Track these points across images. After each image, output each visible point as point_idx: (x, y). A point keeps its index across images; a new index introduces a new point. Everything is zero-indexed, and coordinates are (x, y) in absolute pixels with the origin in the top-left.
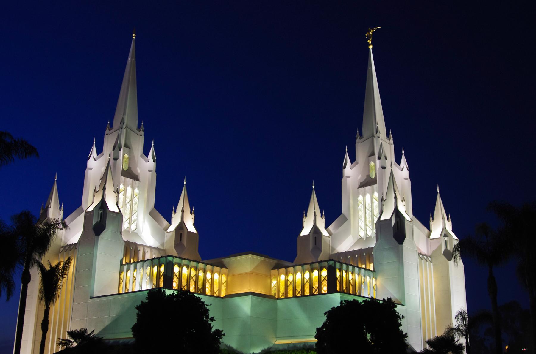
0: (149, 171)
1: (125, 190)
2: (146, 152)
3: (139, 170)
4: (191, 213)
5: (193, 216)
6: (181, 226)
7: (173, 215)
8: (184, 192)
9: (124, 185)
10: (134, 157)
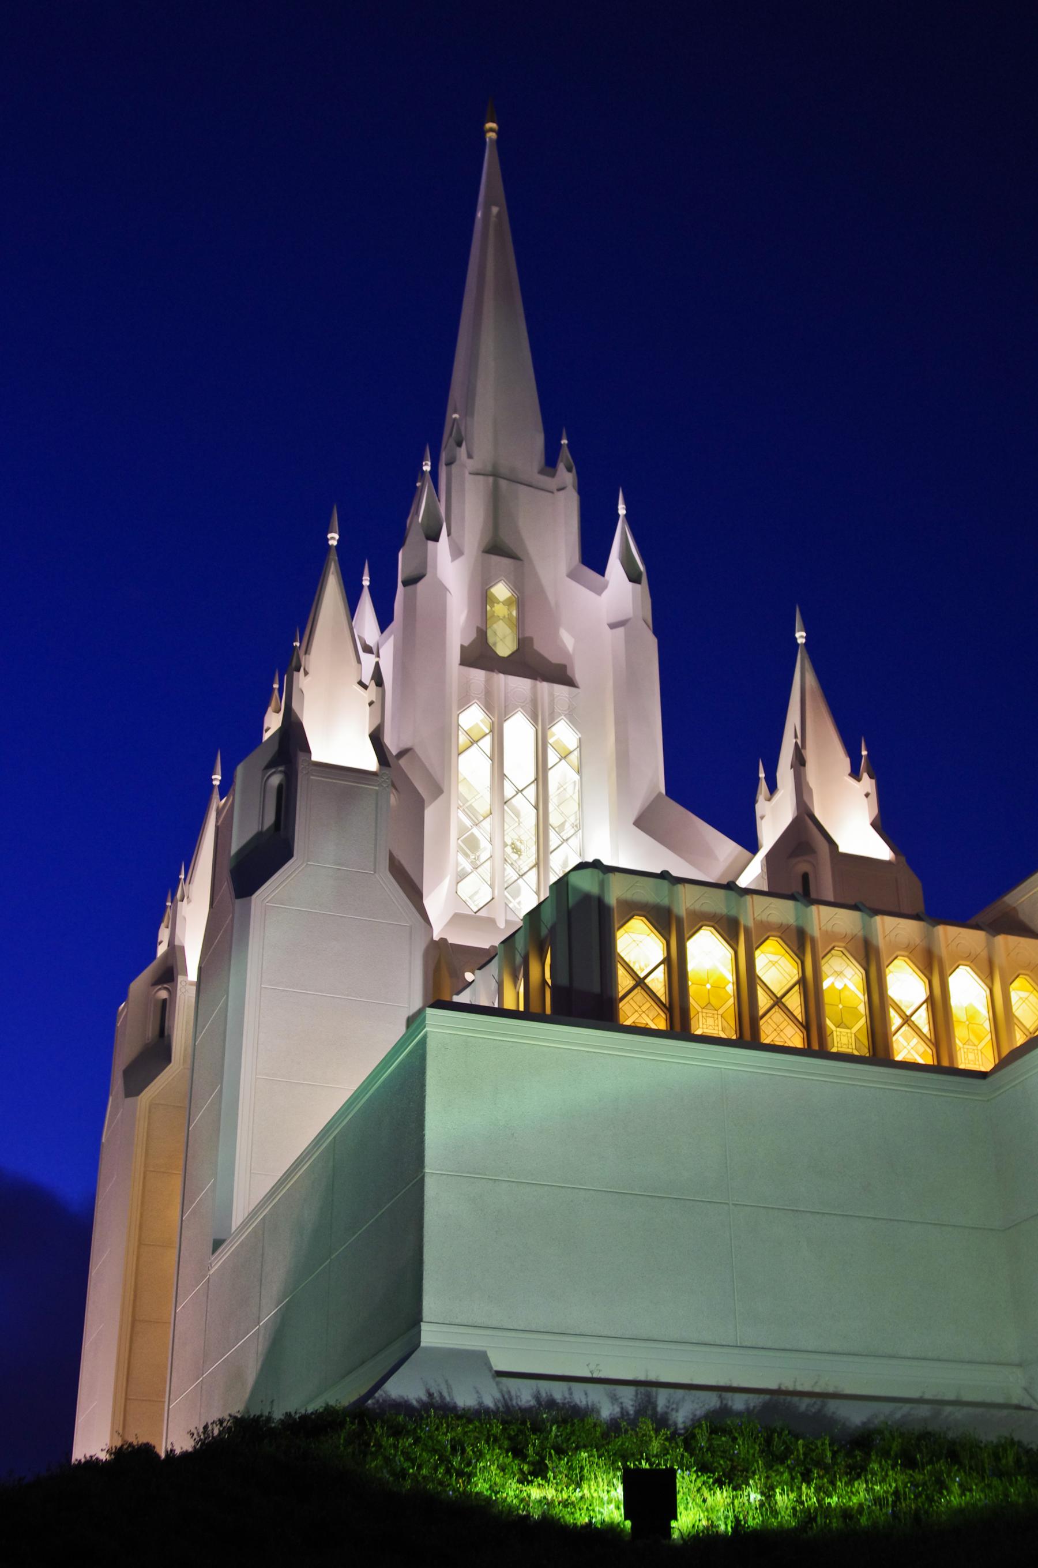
0: (613, 626)
2: (594, 556)
3: (568, 640)
4: (855, 774)
5: (868, 784)
6: (805, 834)
7: (762, 806)
8: (803, 680)
9: (488, 707)
10: (540, 590)
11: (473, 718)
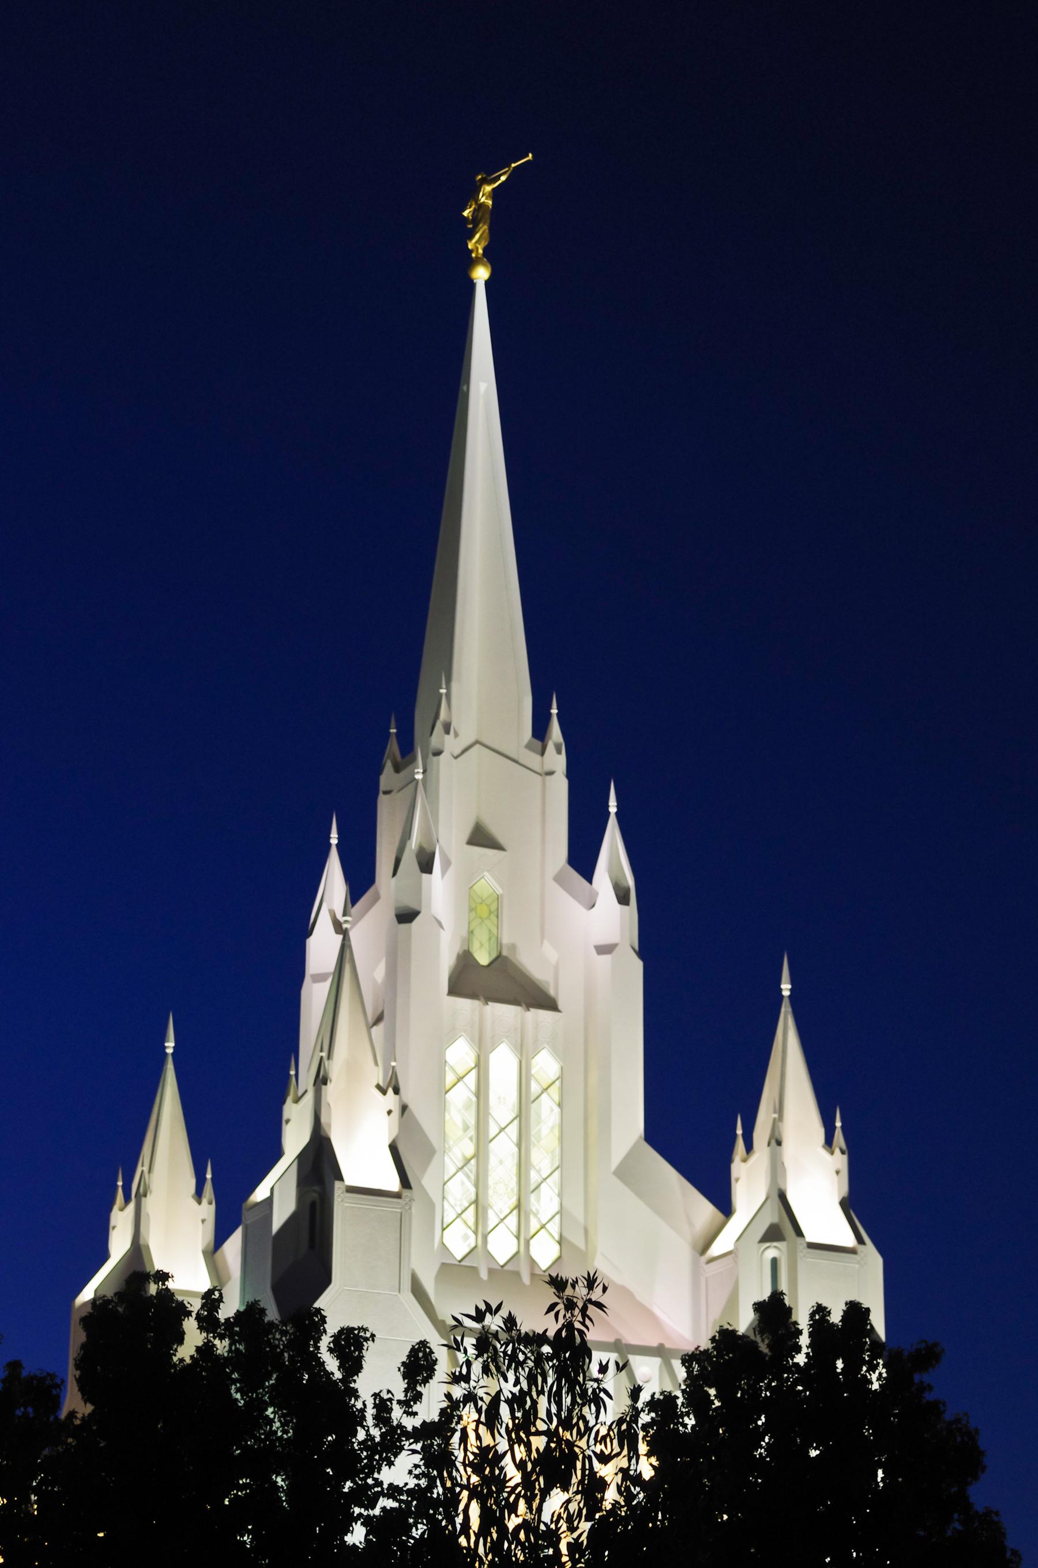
1: (481, 1066)
2: (583, 858)
5: (839, 1161)
7: (739, 1169)
11: (460, 1054)
